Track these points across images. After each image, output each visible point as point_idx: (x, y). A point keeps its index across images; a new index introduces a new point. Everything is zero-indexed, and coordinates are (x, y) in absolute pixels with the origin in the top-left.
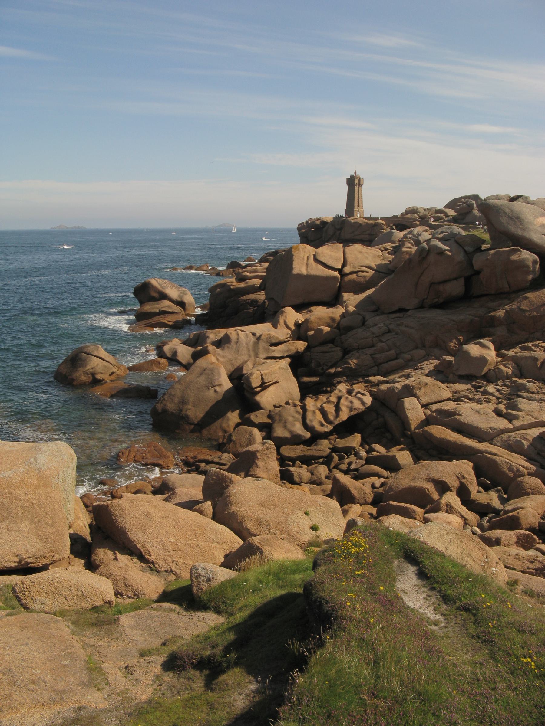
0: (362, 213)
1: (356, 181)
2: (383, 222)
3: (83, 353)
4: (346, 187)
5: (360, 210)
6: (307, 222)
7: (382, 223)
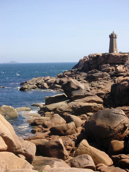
0: (117, 52)
1: (114, 36)
2: (128, 55)
3: (113, 113)
4: (109, 39)
5: (116, 49)
6: (89, 56)
7: (127, 55)
